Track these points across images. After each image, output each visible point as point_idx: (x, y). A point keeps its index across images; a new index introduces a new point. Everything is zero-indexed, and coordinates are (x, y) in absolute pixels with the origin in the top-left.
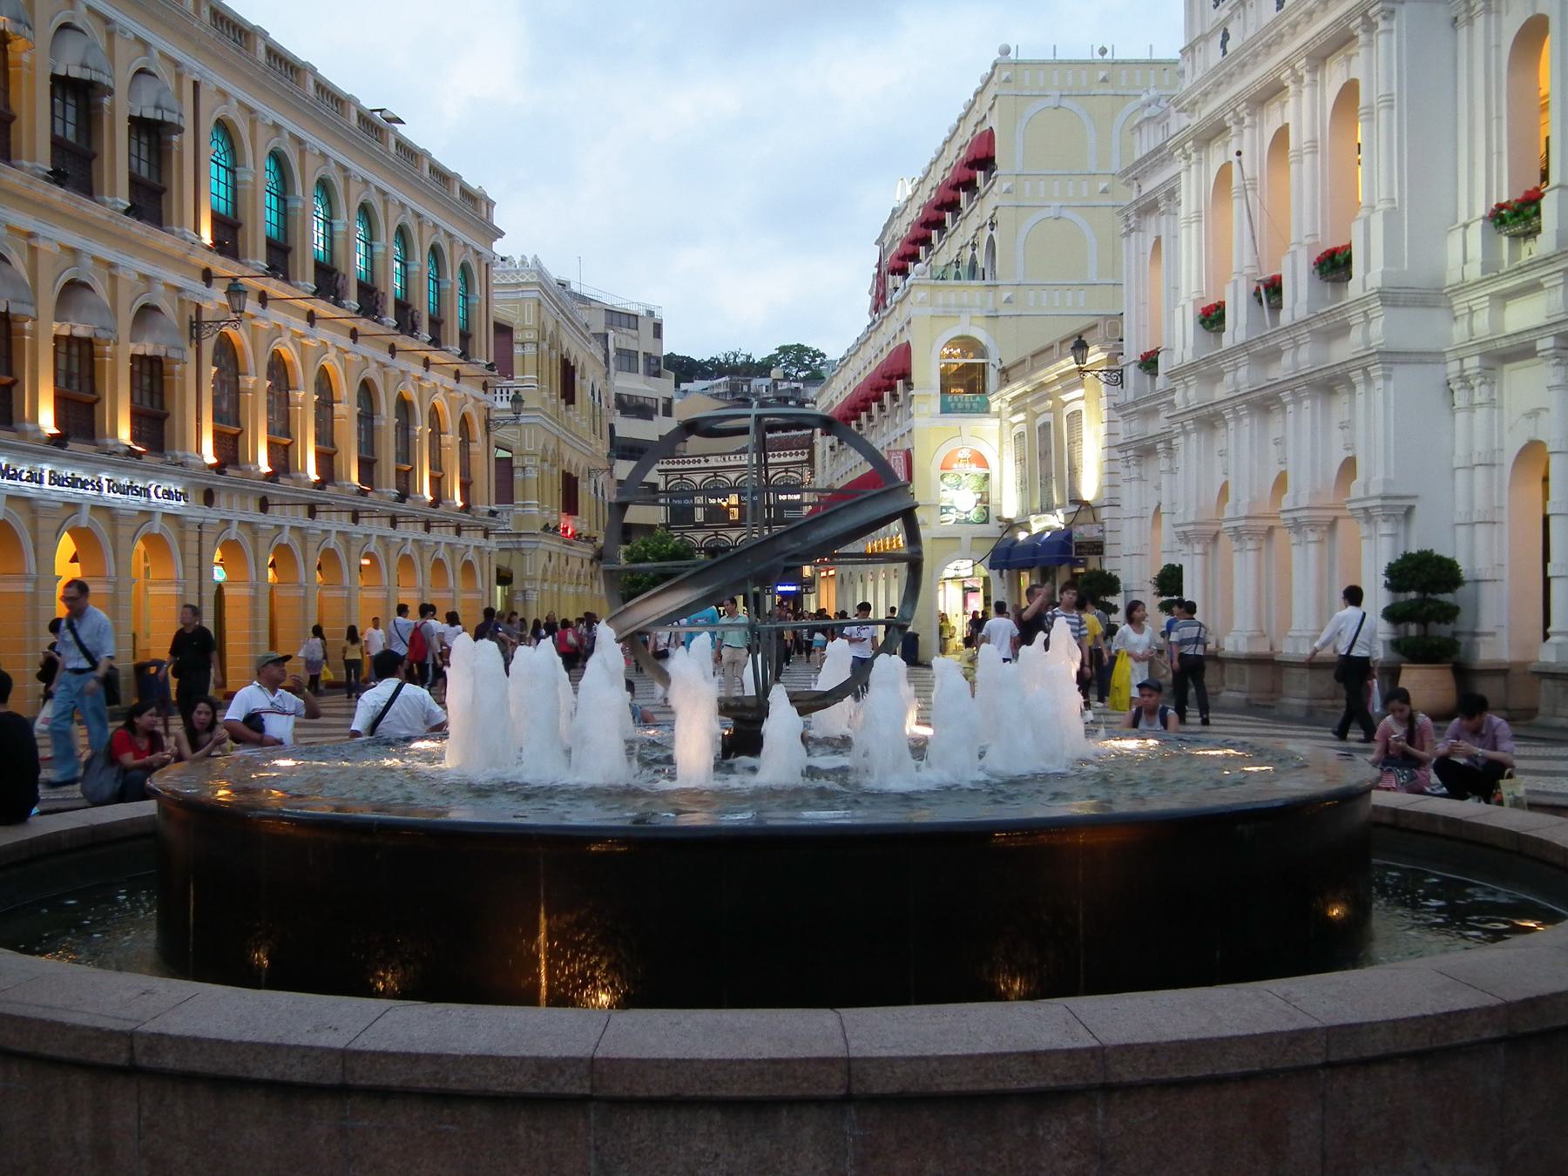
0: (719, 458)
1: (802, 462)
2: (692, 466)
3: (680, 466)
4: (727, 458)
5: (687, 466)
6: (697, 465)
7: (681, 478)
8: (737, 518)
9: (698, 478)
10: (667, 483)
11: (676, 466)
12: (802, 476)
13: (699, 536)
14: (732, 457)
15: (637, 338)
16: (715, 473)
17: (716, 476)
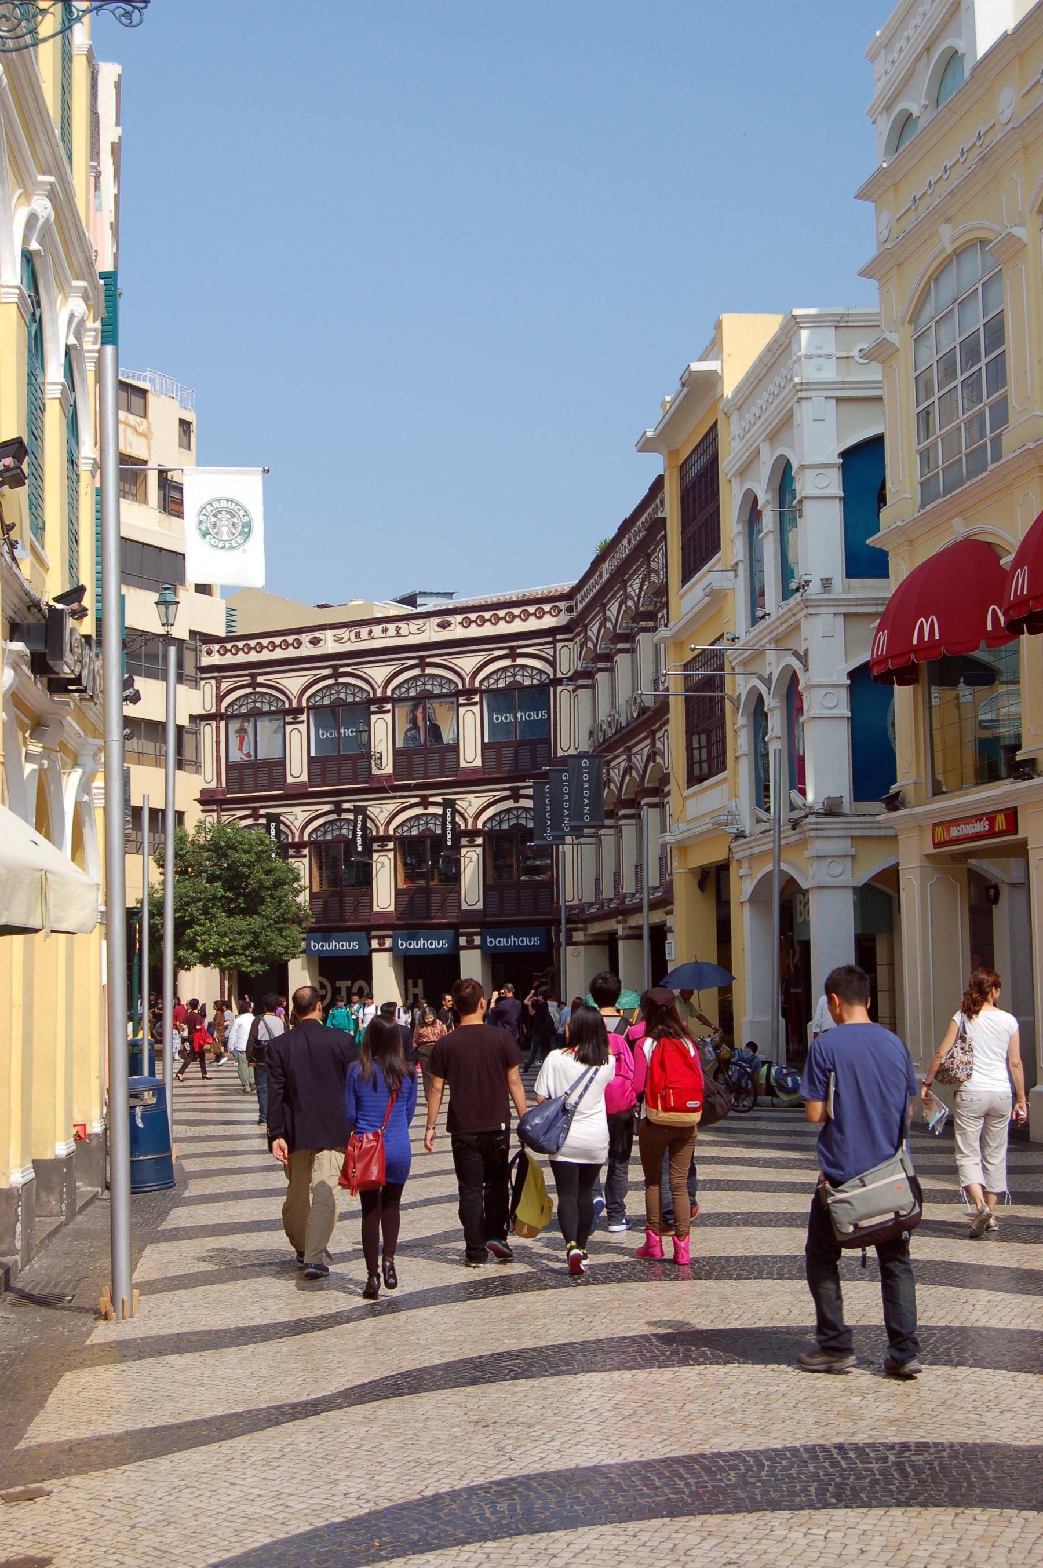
0: (344, 633)
1: (552, 632)
2: (279, 654)
3: (253, 657)
4: (364, 632)
5: (266, 656)
6: (291, 653)
7: (254, 684)
8: (389, 769)
9: (293, 683)
10: (220, 698)
11: (241, 658)
12: (553, 664)
13: (296, 816)
14: (377, 630)
15: (145, 435)
16: (335, 668)
17: (336, 675)
